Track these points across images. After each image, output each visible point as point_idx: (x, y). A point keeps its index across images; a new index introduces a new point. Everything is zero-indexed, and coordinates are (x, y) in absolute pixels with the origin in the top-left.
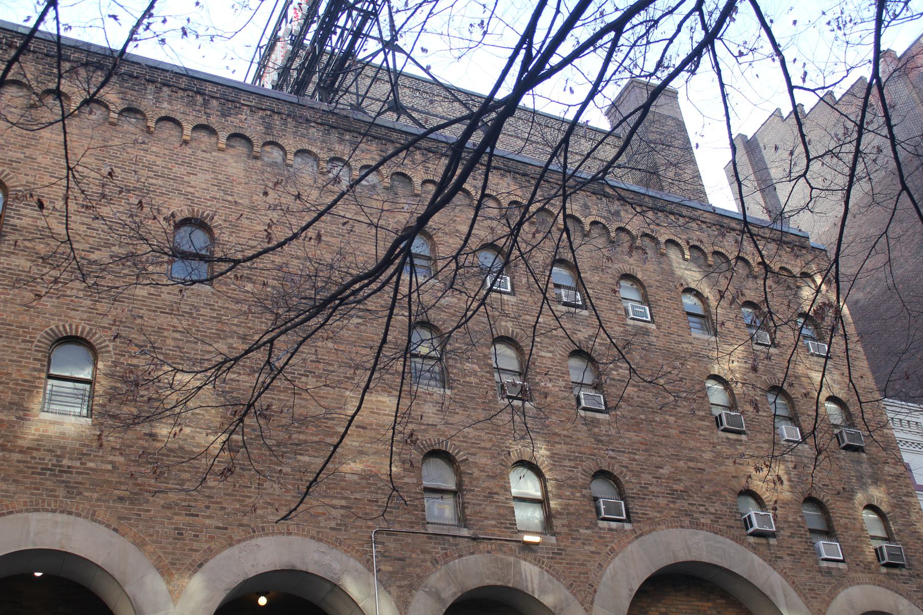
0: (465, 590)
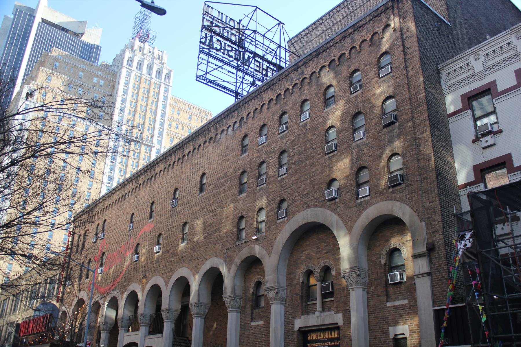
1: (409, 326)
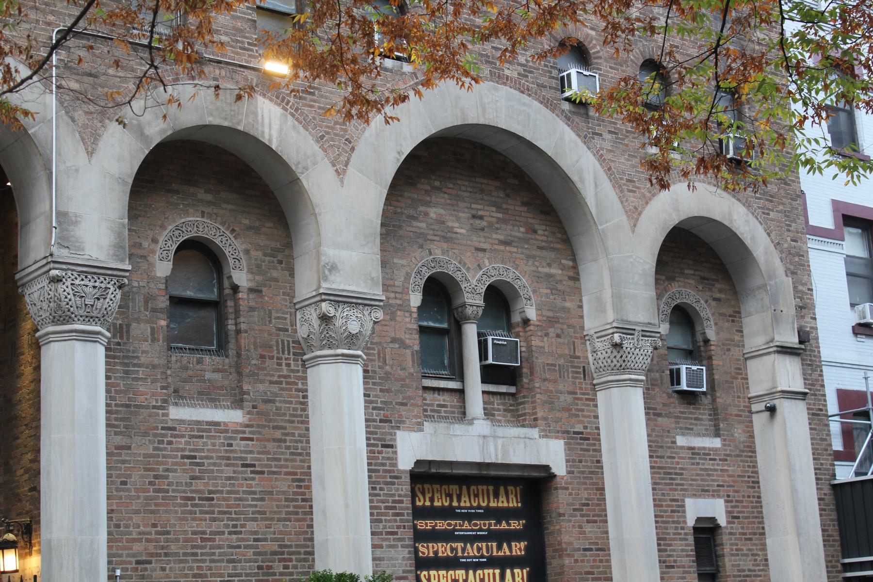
0: (178, 128)
1: (726, 501)
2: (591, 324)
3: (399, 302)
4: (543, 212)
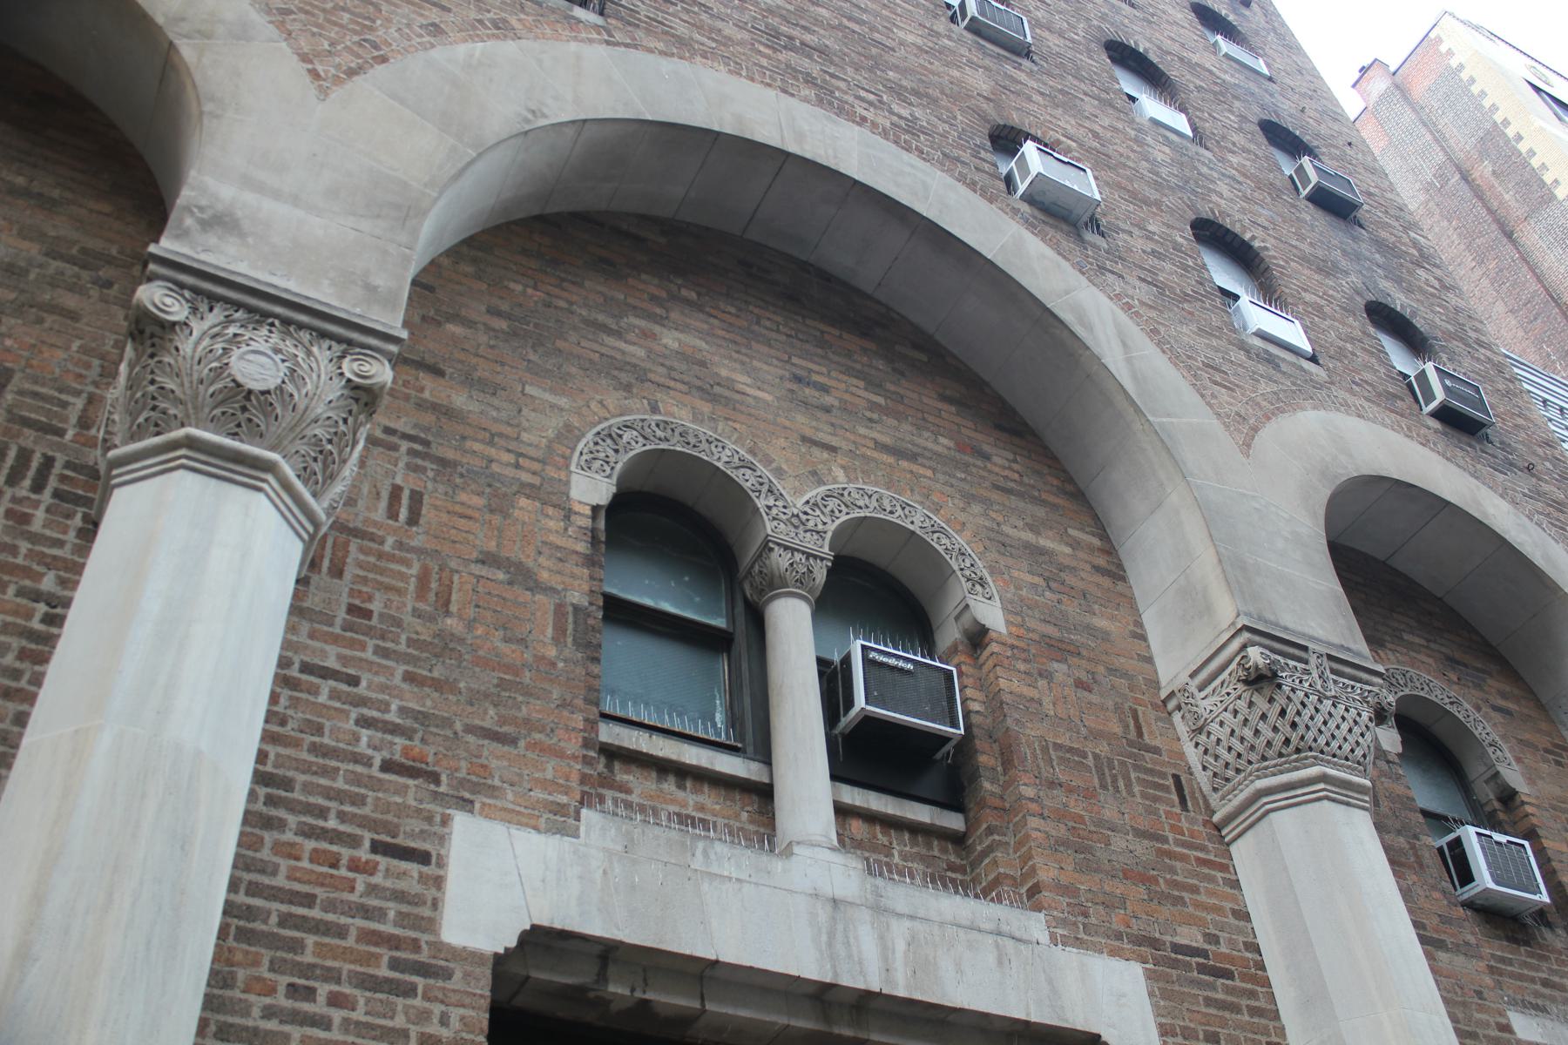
2: (1172, 668)
3: (526, 477)
4: (999, 427)
